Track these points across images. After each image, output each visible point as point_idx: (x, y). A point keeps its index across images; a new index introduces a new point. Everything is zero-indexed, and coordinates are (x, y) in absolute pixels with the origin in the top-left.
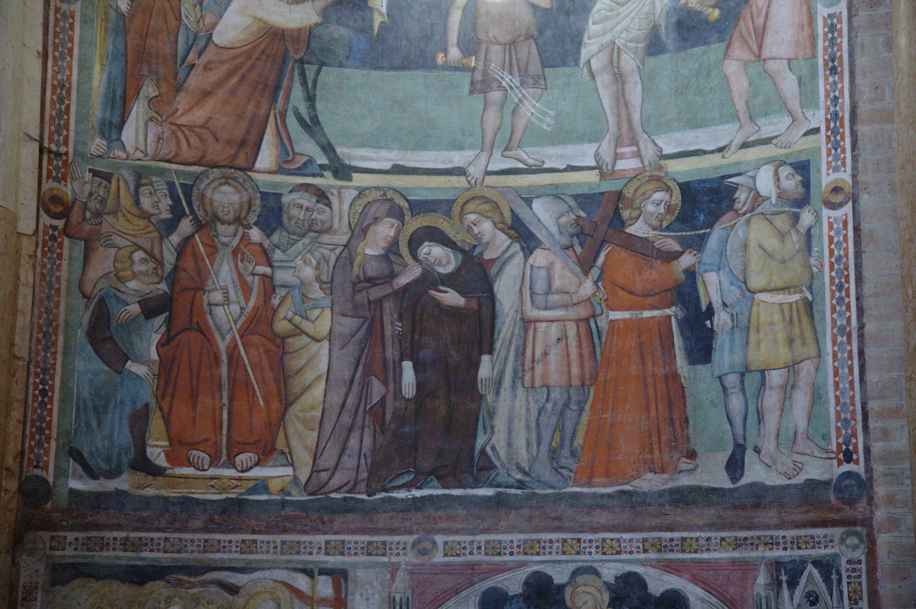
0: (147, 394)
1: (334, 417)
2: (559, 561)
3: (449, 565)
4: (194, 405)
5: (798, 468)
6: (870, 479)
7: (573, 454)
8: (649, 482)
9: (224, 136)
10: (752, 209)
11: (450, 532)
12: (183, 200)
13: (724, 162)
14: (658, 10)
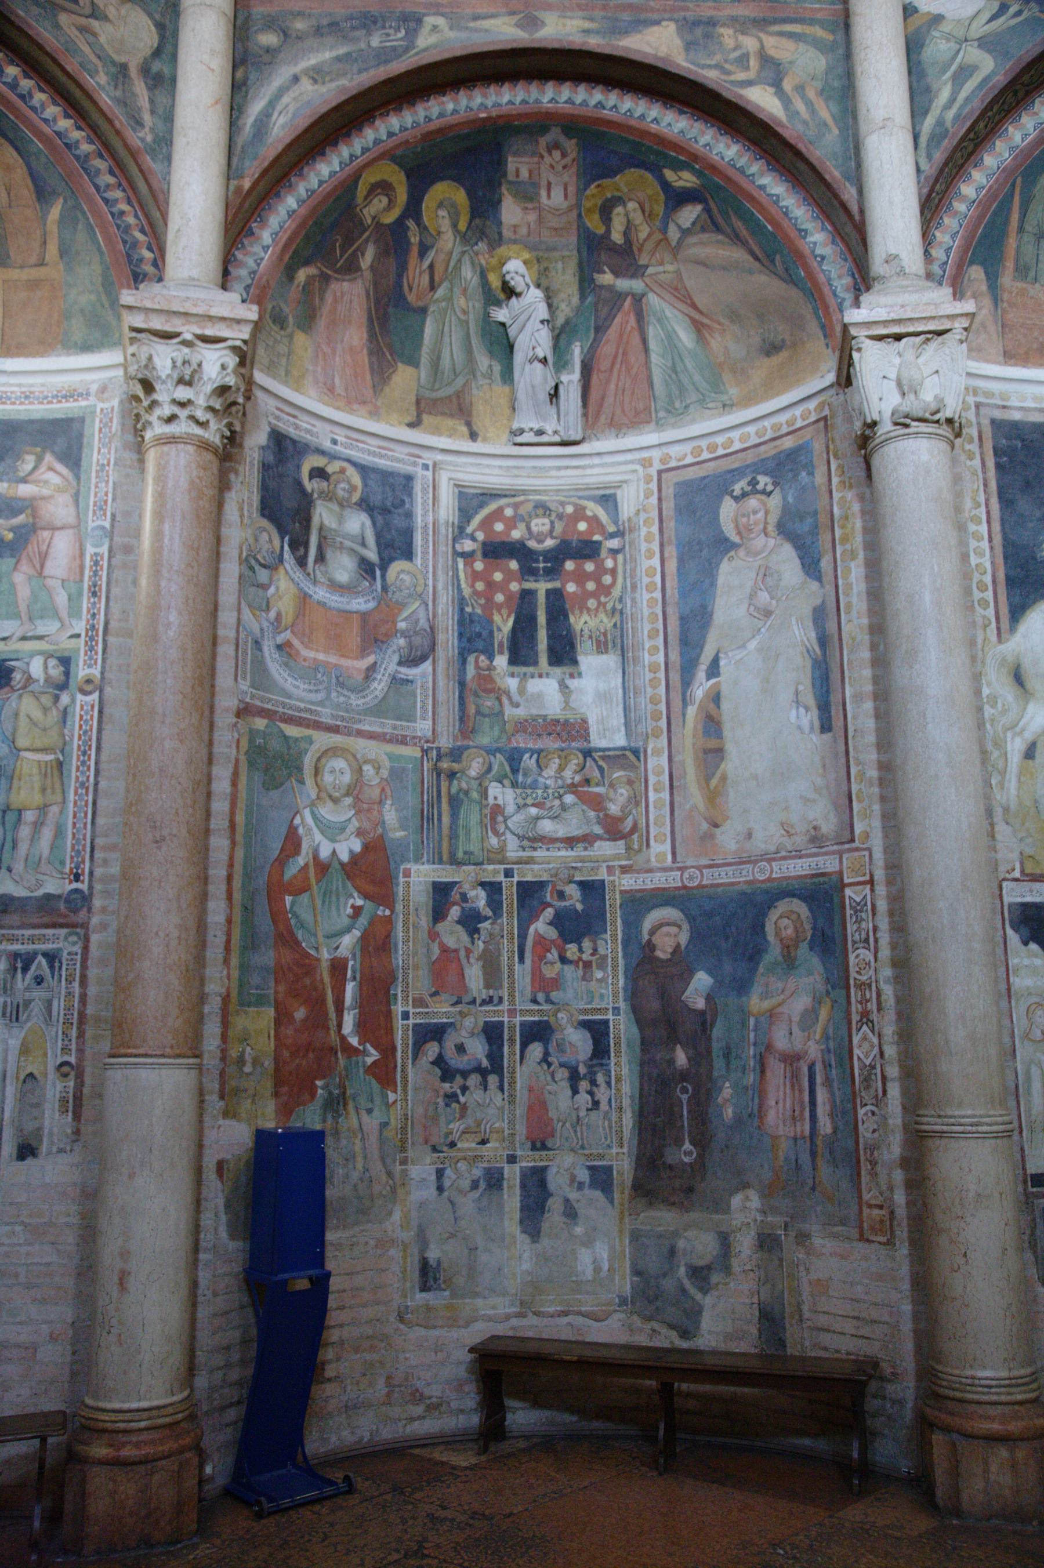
5: (39, 884)
6: (91, 894)
10: (25, 687)
13: (6, 648)
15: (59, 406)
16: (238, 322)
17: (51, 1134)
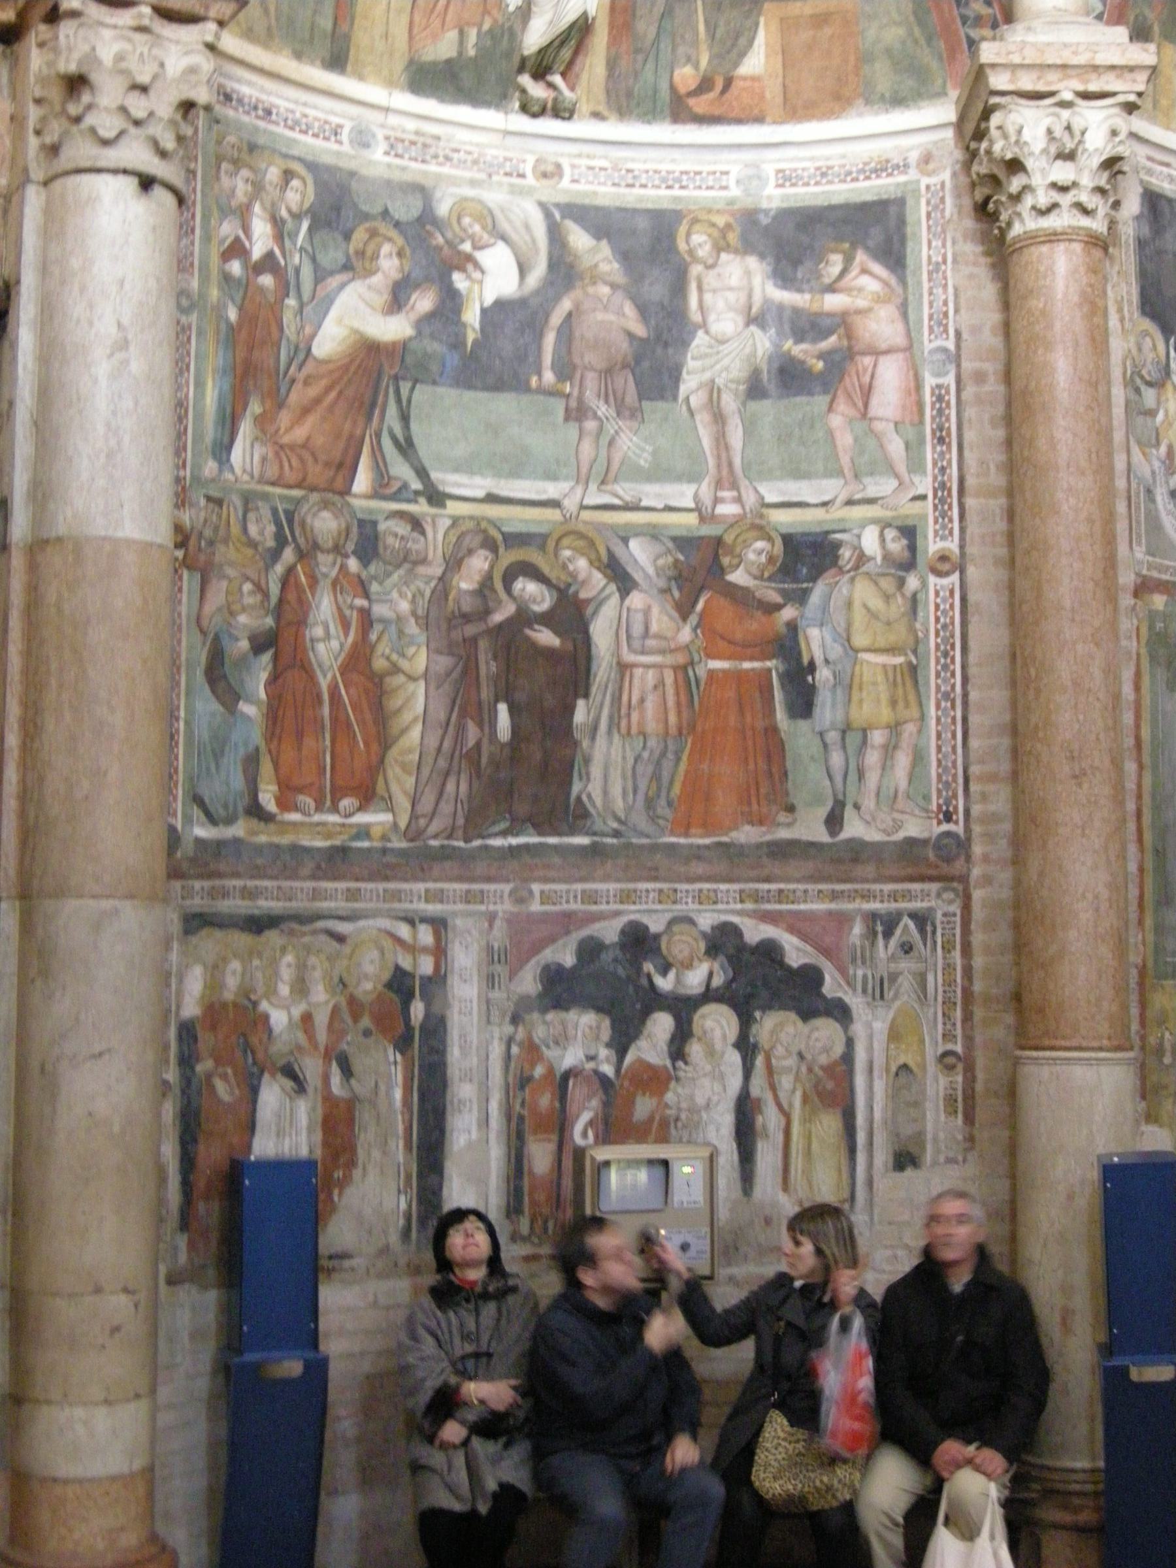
0: (257, 736)
1: (431, 761)
2: (656, 911)
3: (545, 914)
4: (300, 749)
5: (898, 826)
6: (969, 839)
7: (670, 804)
8: (747, 834)
9: (323, 457)
10: (856, 567)
11: (546, 880)
12: (288, 525)
13: (828, 517)
14: (760, 353)
15: (867, 183)
16: (1131, 69)
17: (935, 1140)
